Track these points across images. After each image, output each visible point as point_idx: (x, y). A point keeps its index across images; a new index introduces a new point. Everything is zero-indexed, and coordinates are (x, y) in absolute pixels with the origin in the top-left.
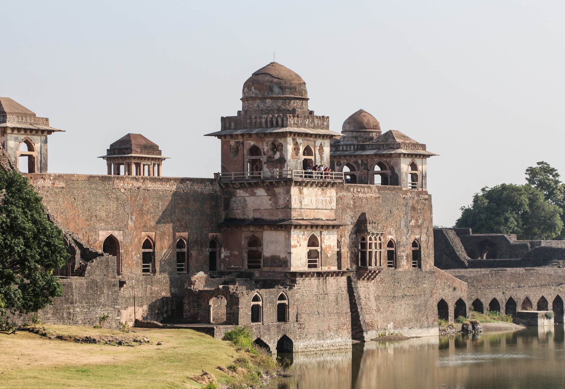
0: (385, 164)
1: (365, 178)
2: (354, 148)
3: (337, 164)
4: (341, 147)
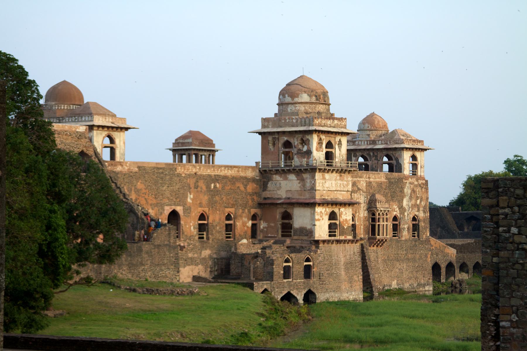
4: (357, 142)
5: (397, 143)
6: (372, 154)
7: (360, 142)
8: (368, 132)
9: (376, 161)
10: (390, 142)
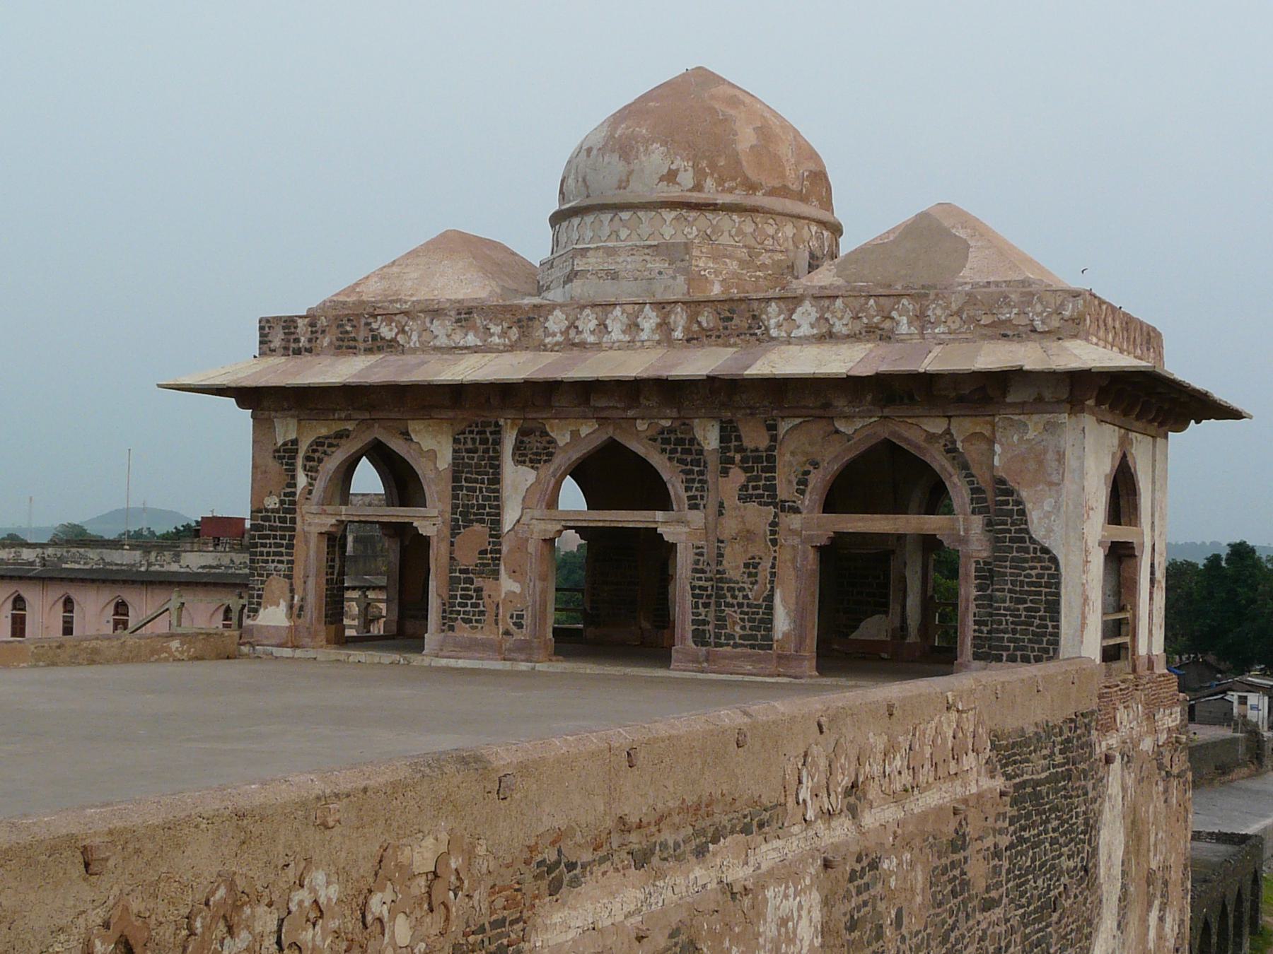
0: (938, 460)
1: (751, 566)
2: (664, 326)
3: (519, 448)
4: (557, 322)
5: (1004, 332)
6: (709, 437)
7: (588, 322)
8: (668, 227)
9: (757, 516)
10: (921, 318)
